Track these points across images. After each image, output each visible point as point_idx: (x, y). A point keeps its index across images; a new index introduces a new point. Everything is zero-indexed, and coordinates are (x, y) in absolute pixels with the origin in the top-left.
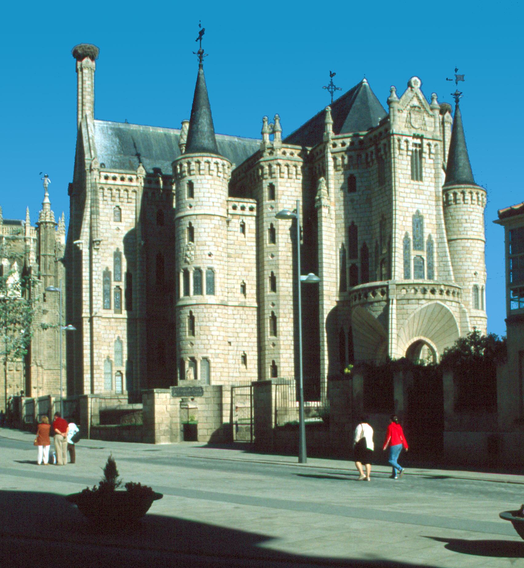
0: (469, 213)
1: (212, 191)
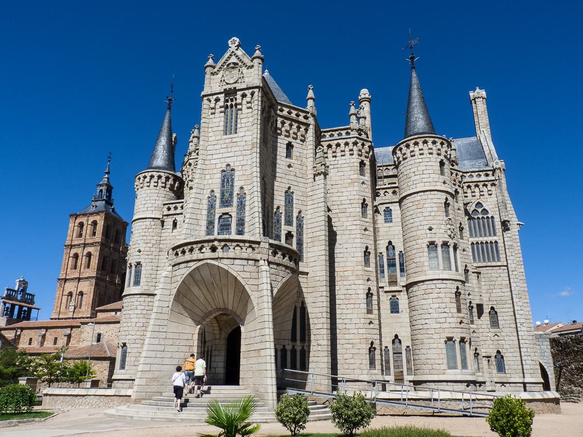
0: (417, 165)
1: (148, 198)
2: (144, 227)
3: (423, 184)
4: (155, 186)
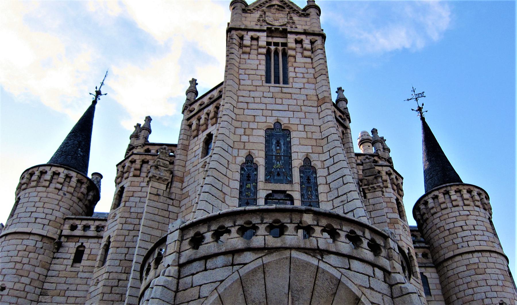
1: (41, 204)
2: (19, 248)
3: (477, 243)
4: (56, 188)
